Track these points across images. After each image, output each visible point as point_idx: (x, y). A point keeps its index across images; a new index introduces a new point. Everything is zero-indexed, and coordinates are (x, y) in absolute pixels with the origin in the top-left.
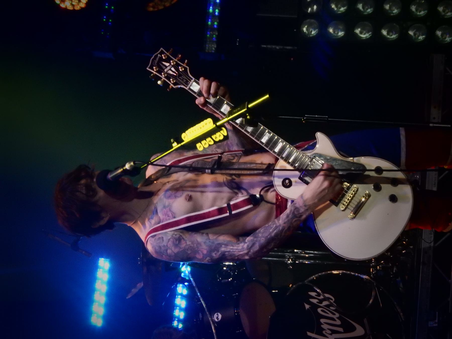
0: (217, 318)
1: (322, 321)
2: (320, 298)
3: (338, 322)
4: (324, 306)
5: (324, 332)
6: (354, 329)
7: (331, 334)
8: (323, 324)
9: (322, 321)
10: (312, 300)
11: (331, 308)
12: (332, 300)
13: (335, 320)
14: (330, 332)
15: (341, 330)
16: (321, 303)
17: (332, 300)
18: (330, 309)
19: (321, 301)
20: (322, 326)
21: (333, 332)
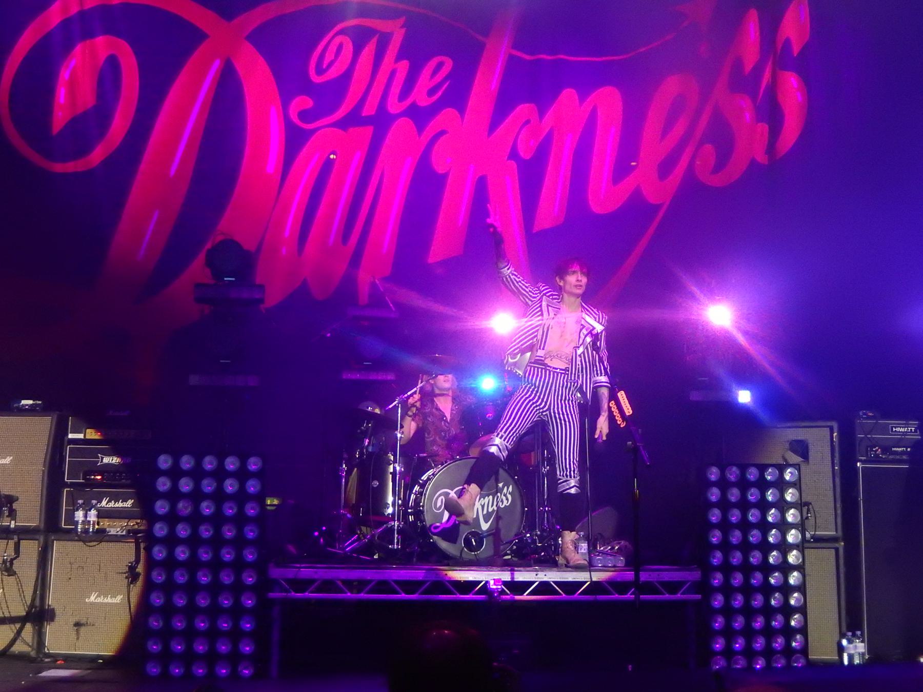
0: (489, 416)
1: (491, 497)
2: (508, 494)
3: (490, 510)
4: (502, 499)
5: (482, 499)
6: (486, 522)
7: (481, 504)
8: (488, 497)
9: (491, 497)
10: (506, 487)
11: (501, 503)
12: (507, 503)
13: (492, 506)
14: (482, 504)
15: (485, 512)
16: (504, 495)
17: (507, 503)
18: (501, 501)
19: (505, 495)
20: (487, 497)
21: (483, 507)
